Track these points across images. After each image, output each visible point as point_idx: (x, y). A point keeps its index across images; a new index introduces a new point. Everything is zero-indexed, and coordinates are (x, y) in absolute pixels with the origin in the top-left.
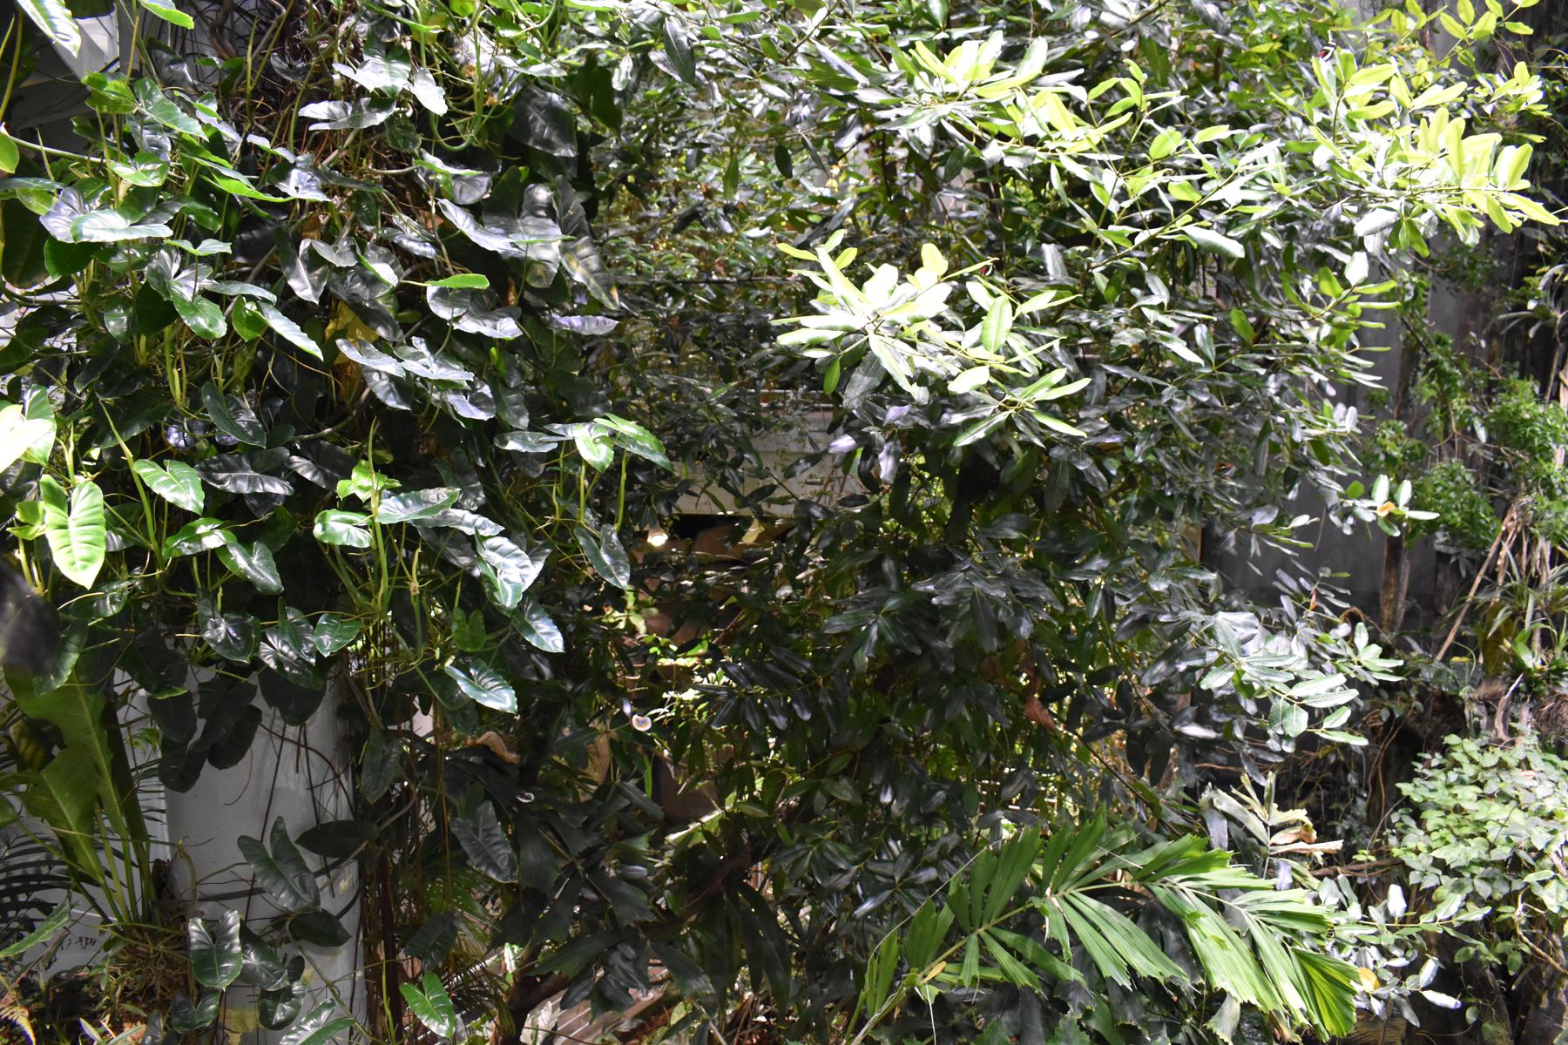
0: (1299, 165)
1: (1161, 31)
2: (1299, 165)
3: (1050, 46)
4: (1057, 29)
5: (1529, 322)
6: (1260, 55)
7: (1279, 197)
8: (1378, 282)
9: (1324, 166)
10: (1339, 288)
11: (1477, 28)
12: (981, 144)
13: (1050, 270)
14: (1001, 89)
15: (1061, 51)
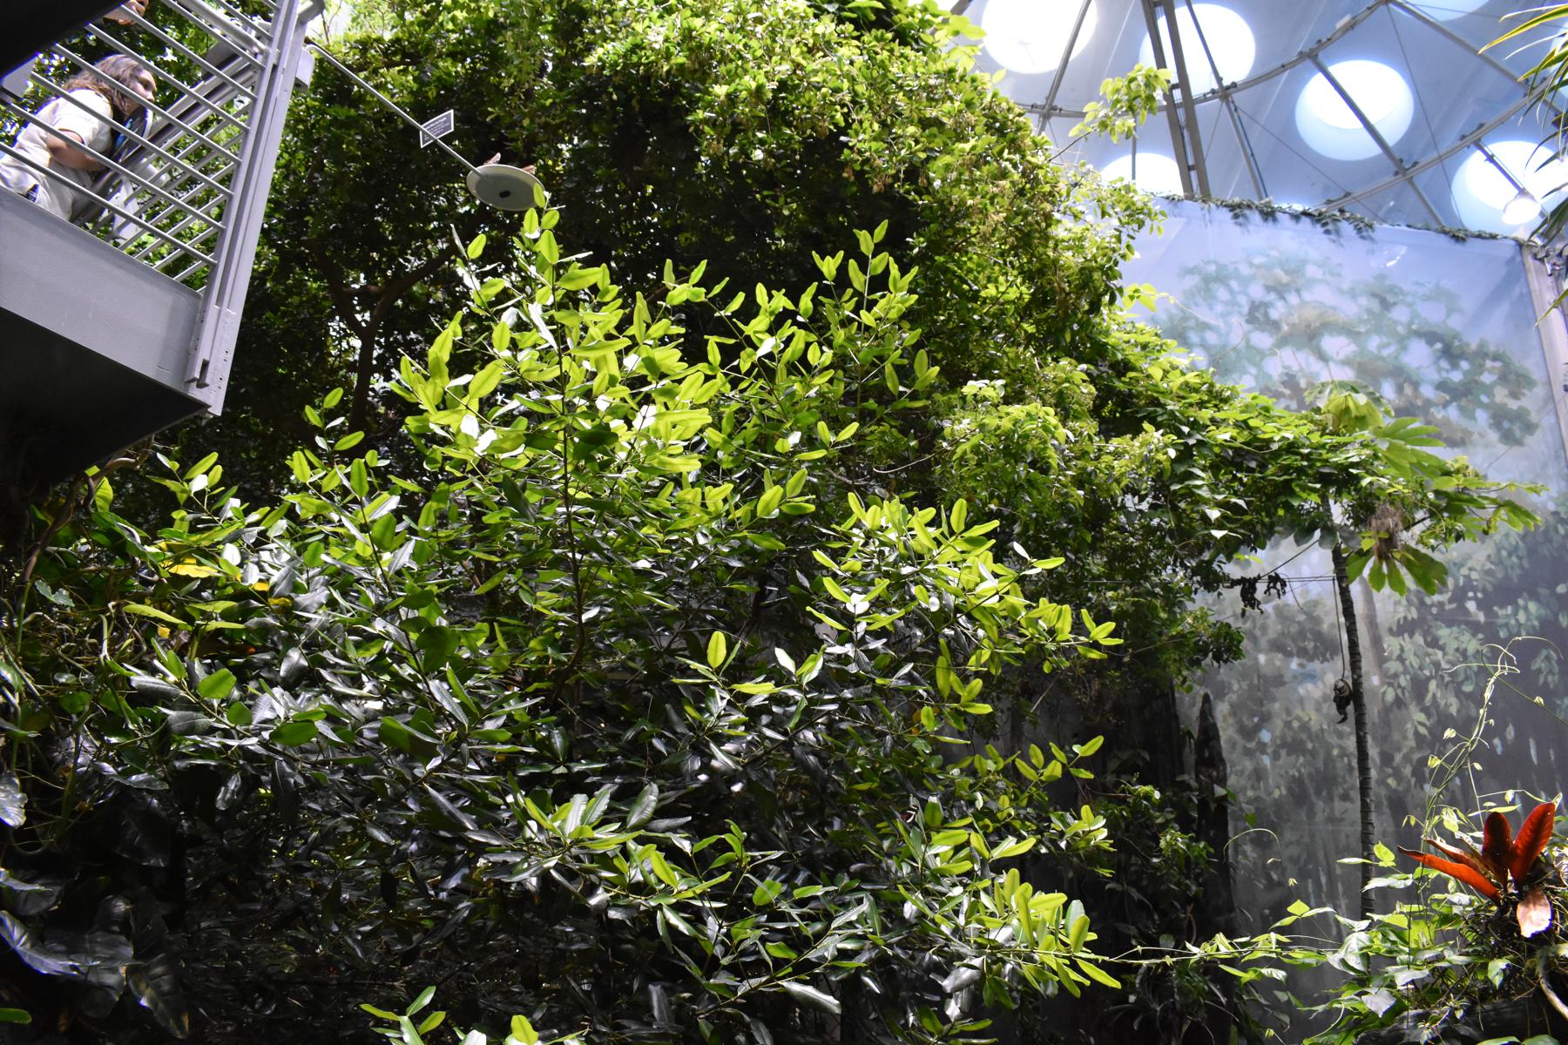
0: (890, 910)
1: (767, 776)
2: (890, 910)
3: (661, 791)
4: (668, 773)
5: (1132, 1013)
6: (860, 792)
7: (875, 946)
8: (977, 1019)
9: (914, 921)
10: (939, 1025)
11: (1047, 772)
12: (591, 890)
13: (656, 1013)
14: (608, 839)
15: (672, 795)
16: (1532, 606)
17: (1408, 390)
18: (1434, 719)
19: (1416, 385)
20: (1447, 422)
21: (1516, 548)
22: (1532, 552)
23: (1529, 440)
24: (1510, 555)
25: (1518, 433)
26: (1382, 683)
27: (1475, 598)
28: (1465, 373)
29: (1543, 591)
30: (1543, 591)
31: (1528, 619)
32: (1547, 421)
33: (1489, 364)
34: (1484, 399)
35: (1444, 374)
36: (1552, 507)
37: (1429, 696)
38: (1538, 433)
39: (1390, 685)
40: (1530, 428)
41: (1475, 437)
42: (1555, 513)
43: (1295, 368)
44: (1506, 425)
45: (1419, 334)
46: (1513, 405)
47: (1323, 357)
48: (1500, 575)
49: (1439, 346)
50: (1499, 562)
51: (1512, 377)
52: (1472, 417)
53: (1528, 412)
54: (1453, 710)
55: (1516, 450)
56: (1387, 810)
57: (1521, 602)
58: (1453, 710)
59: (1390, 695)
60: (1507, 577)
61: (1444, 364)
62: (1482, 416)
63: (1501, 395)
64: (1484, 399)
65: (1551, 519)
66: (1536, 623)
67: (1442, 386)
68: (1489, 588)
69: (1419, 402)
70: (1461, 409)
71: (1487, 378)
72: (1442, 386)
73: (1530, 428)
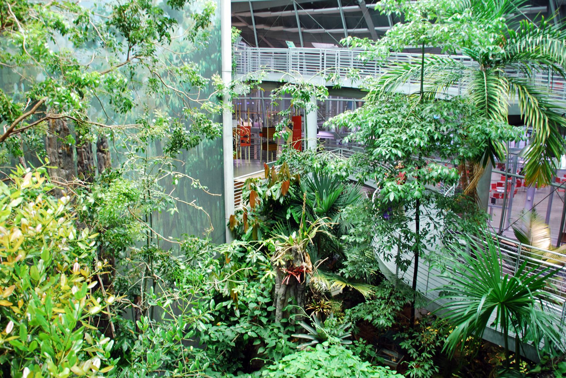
16: (204, 63)
18: (171, 109)
26: (156, 97)
30: (207, 57)
31: (202, 68)
37: (170, 100)
39: (158, 97)
48: (196, 51)
54: (177, 105)
56: (154, 145)
57: (201, 62)
58: (177, 105)
59: (158, 103)
60: (198, 52)
66: (204, 70)
68: (192, 57)
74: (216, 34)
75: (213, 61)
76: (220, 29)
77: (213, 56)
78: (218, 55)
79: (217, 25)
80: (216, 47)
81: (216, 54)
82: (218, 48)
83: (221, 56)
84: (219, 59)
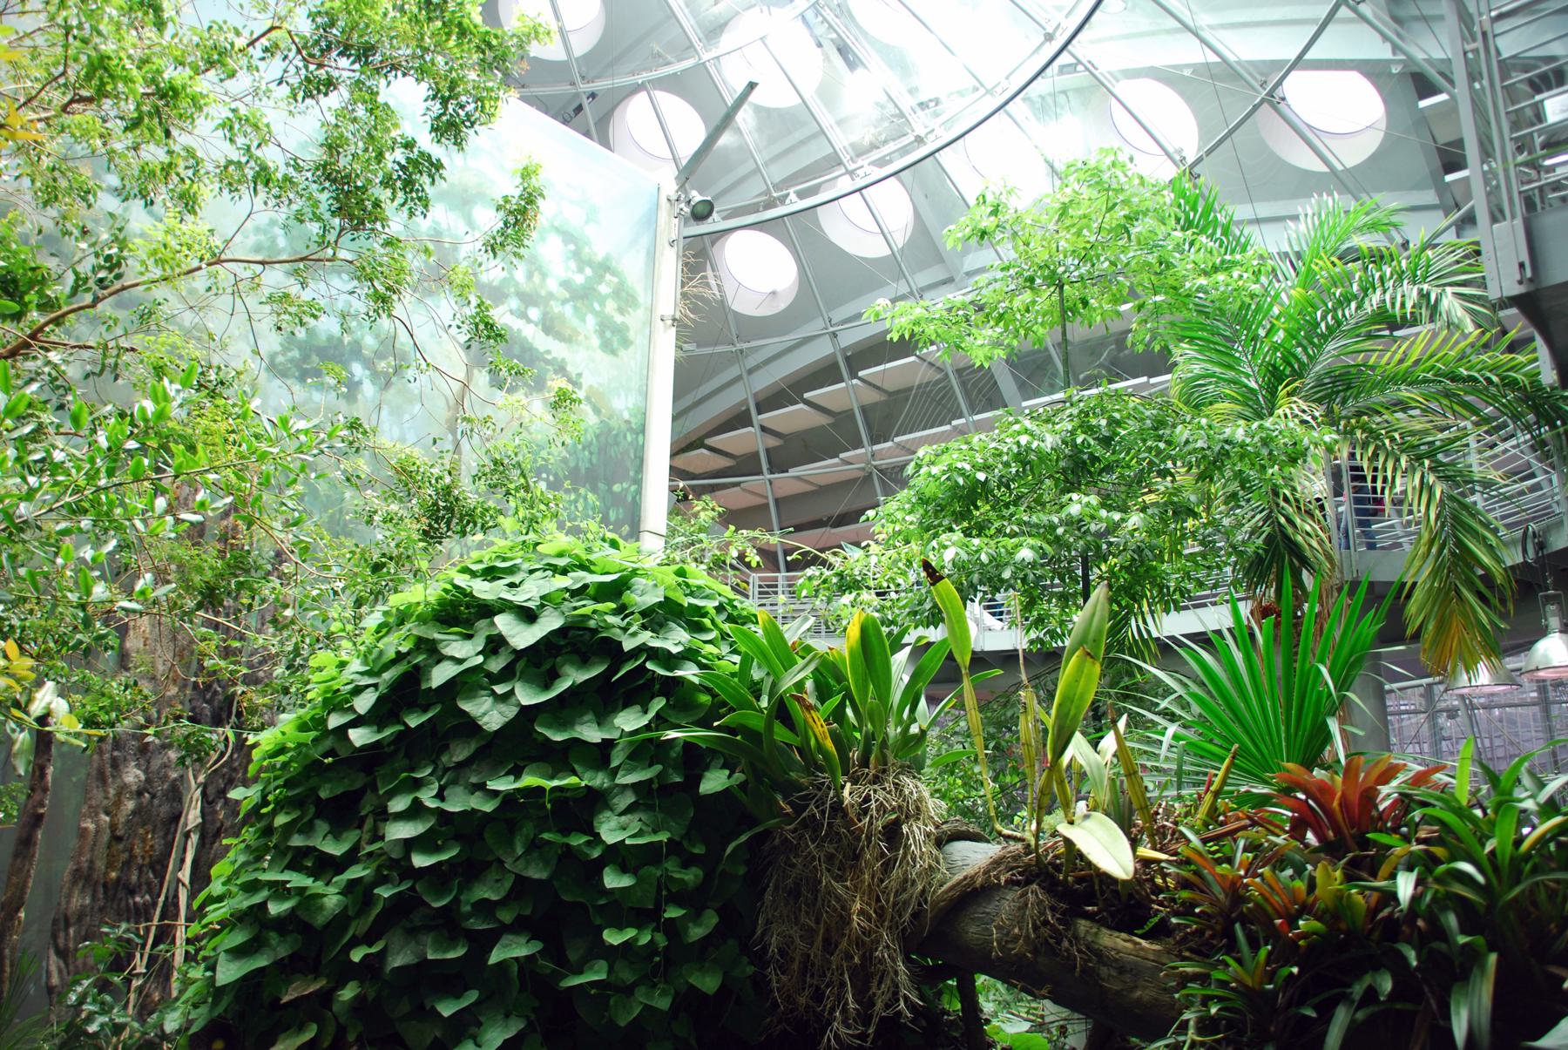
17: (537, 278)
19: (544, 276)
20: (561, 316)
21: (591, 444)
22: (602, 450)
23: (622, 352)
24: (584, 448)
25: (615, 345)
27: (547, 480)
28: (588, 279)
29: (601, 486)
32: (639, 340)
33: (608, 277)
34: (597, 306)
35: (570, 275)
36: (626, 416)
38: (631, 349)
40: (626, 343)
41: (581, 338)
42: (628, 422)
43: (444, 226)
44: (608, 334)
45: (557, 230)
46: (618, 319)
47: (470, 222)
48: (572, 464)
49: (572, 247)
50: (574, 453)
51: (624, 294)
52: (583, 320)
53: (628, 329)
55: (609, 358)
57: (582, 491)
60: (577, 467)
61: (573, 265)
62: (591, 321)
63: (611, 307)
64: (597, 306)
65: (624, 427)
67: (566, 284)
69: (543, 293)
70: (575, 308)
71: (603, 289)
72: (566, 284)
73: (626, 343)
74: (629, 438)
75: (617, 500)
76: (643, 430)
77: (617, 488)
78: (633, 488)
79: (633, 420)
80: (628, 471)
81: (625, 485)
82: (632, 473)
83: (639, 492)
84: (634, 498)
